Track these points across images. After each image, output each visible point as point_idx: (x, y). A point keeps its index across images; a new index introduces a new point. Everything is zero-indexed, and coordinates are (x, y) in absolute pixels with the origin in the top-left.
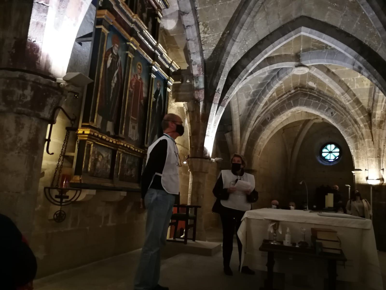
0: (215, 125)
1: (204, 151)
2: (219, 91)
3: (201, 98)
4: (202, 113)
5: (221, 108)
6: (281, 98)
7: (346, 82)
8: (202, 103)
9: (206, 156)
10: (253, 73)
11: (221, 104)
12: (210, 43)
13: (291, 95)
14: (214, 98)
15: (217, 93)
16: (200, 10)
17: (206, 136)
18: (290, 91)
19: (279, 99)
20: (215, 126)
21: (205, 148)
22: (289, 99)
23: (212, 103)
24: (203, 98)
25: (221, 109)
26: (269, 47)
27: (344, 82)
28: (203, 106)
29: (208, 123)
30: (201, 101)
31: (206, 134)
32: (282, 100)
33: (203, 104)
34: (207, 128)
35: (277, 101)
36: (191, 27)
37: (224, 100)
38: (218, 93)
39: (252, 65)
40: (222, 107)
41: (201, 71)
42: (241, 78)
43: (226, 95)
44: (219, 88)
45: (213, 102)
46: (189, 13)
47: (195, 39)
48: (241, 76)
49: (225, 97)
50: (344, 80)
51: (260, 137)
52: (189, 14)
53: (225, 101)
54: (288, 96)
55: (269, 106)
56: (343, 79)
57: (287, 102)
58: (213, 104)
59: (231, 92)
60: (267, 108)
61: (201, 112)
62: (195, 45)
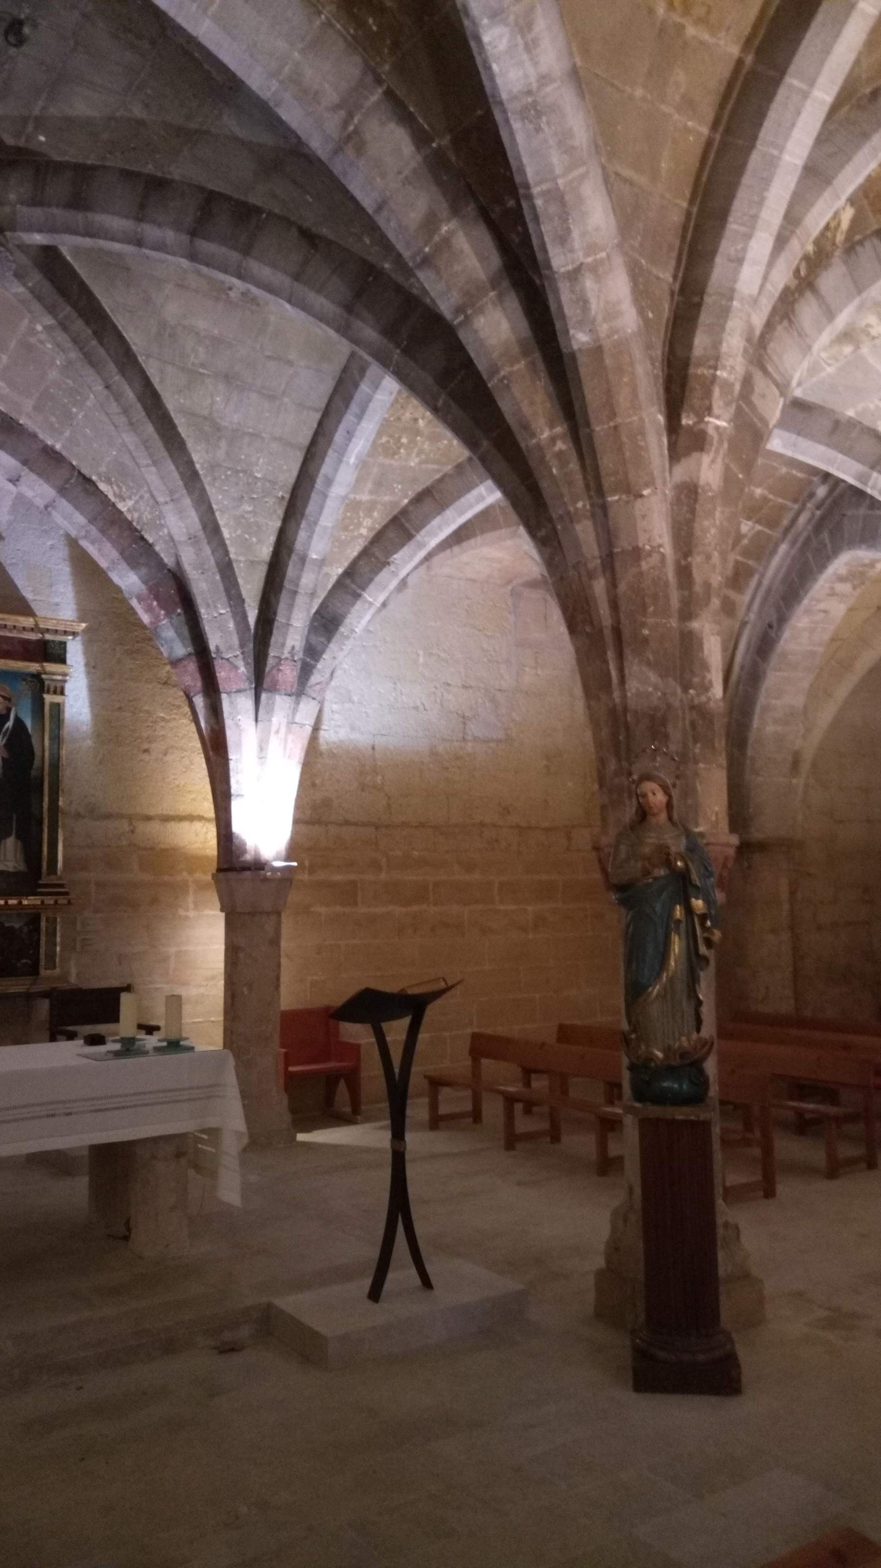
0: (263, 758)
1: (234, 848)
2: (221, 653)
3: (193, 684)
4: (209, 729)
5: (268, 699)
6: (793, 531)
7: (867, 422)
8: (202, 699)
9: (241, 862)
10: (413, 532)
11: (265, 686)
12: (151, 519)
13: (822, 509)
14: (218, 679)
15: (220, 661)
16: (64, 447)
17: (233, 798)
18: (812, 495)
19: (790, 537)
20: (263, 760)
21: (237, 837)
22: (818, 528)
23: (221, 693)
24: (199, 684)
25: (271, 702)
26: (328, 460)
27: (860, 423)
28: (206, 707)
29: (230, 757)
30: (195, 695)
31: (233, 791)
32: (798, 535)
33: (204, 701)
34: (232, 774)
35: (783, 548)
36: (54, 508)
37: (269, 672)
38: (222, 659)
39: (308, 534)
40: (269, 694)
41: (157, 609)
42: (294, 589)
43: (272, 655)
44: (215, 645)
45: (221, 690)
46: (20, 477)
47: (87, 532)
48: (293, 582)
49: (271, 662)
50: (857, 413)
51: (758, 710)
52: (22, 480)
53: (274, 672)
54: (813, 515)
55: (762, 575)
56: (851, 413)
57: (814, 543)
58: (224, 696)
59: (281, 640)
60: (759, 583)
61: (206, 728)
62: (96, 546)
